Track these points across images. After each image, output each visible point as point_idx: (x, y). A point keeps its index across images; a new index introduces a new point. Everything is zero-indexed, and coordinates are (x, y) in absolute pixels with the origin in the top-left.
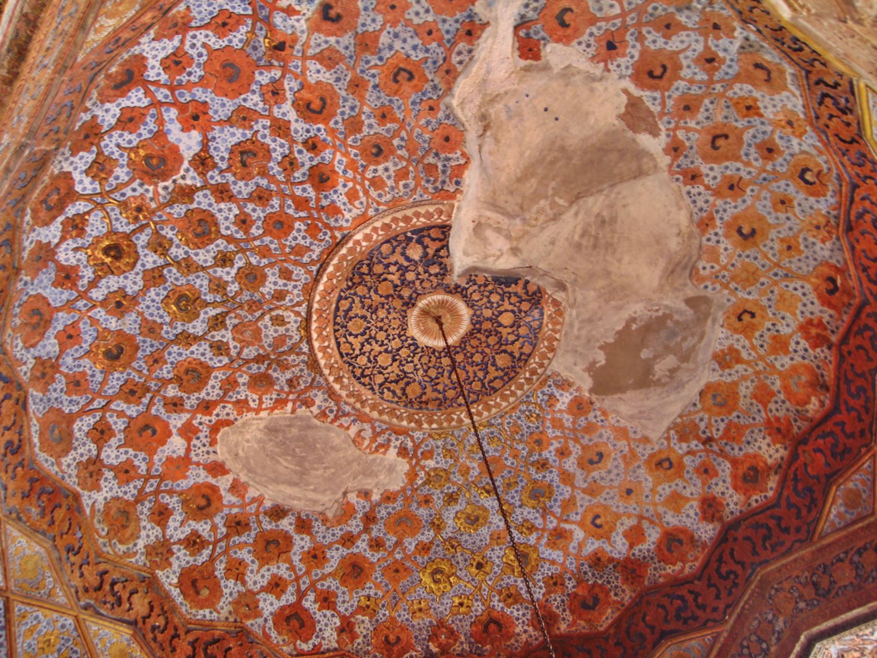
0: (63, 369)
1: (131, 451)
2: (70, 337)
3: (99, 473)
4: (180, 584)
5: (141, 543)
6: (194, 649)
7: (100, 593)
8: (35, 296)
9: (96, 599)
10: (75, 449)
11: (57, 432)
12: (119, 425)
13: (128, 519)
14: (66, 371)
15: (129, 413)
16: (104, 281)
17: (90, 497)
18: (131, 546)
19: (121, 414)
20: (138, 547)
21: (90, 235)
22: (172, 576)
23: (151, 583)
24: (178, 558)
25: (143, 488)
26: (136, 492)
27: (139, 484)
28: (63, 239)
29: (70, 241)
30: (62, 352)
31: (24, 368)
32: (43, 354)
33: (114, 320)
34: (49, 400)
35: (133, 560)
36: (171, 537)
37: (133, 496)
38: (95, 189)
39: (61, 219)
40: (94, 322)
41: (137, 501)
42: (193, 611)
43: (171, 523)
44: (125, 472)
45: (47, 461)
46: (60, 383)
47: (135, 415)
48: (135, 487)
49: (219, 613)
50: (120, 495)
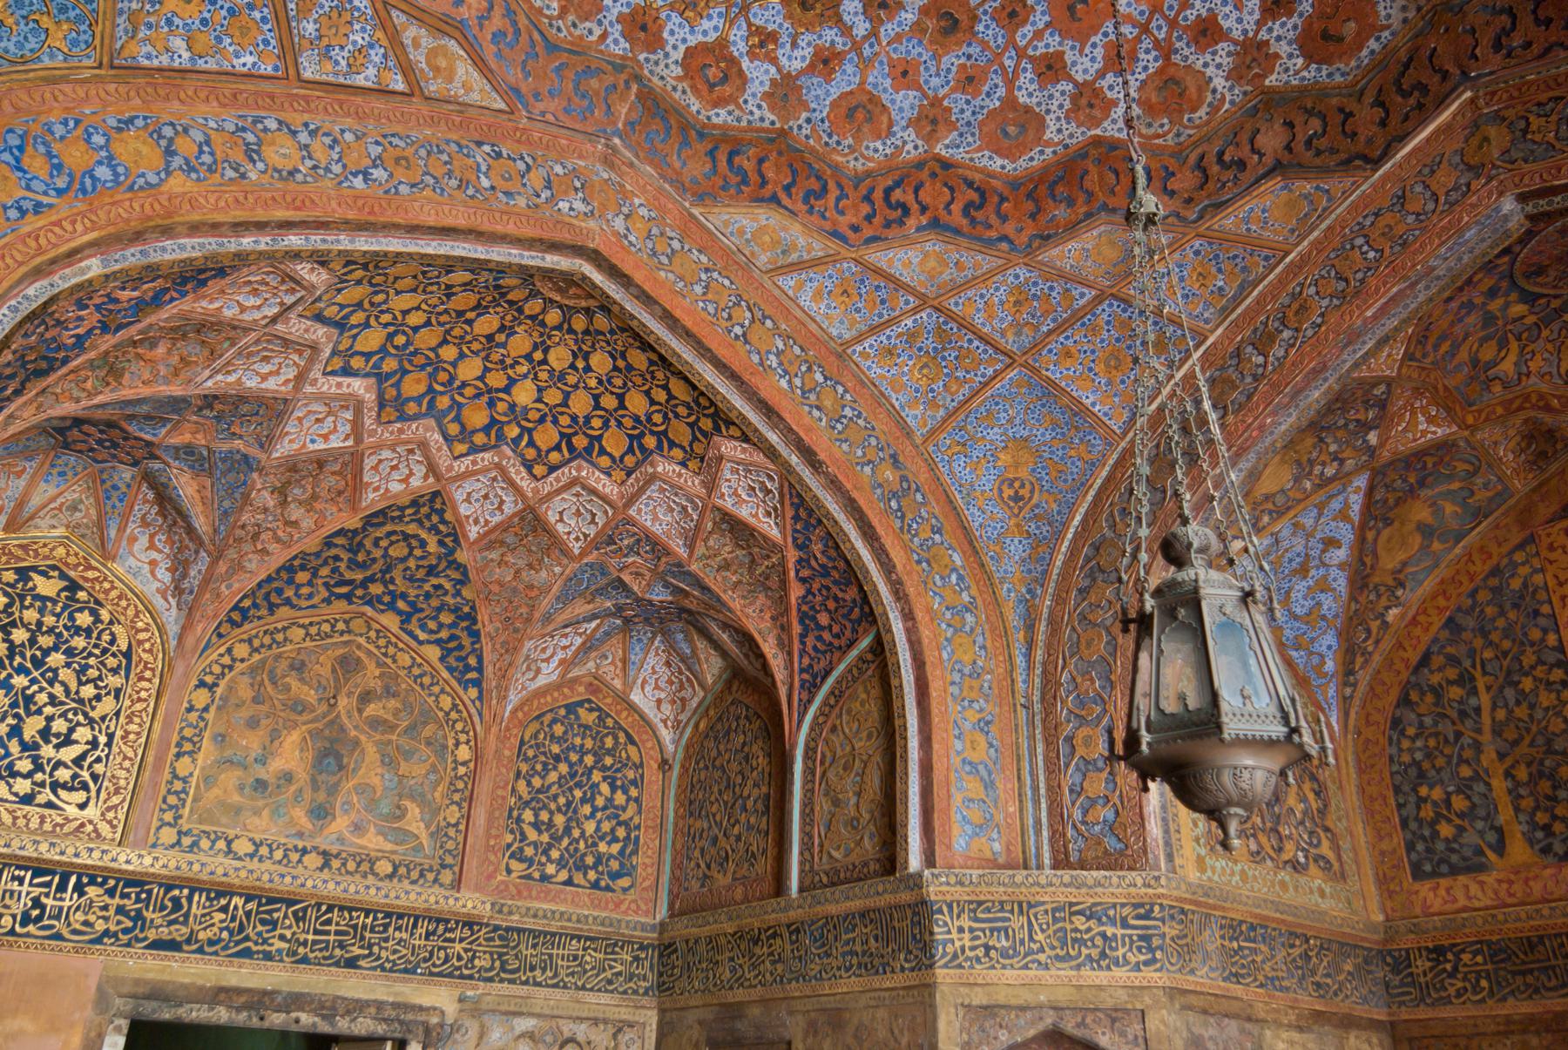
0: (941, 93)
1: (1096, 39)
2: (905, 73)
3: (1098, 93)
4: (1309, 58)
5: (1219, 82)
6: (1382, 104)
7: (1210, 185)
8: (831, 110)
9: (1209, 196)
10: (1048, 112)
11: (1011, 130)
12: (1052, 42)
13: (1177, 83)
14: (947, 88)
15: (1041, 25)
16: (846, 18)
17: (1114, 121)
18: (1209, 98)
19: (1038, 35)
20: (1220, 89)
21: (781, 25)
22: (1290, 64)
23: (1269, 103)
24: (1279, 38)
25: (1157, 42)
26: (1154, 53)
27: (1146, 43)
28: (774, 61)
29: (780, 52)
30: (919, 88)
31: (909, 147)
32: (907, 114)
33: (903, 14)
34: (969, 124)
35: (1227, 106)
36: (1245, 32)
37: (1156, 60)
38: (720, 14)
39: (745, 63)
40: (898, 38)
41: (1167, 58)
42: (1353, 63)
43: (1225, 24)
44: (1118, 59)
45: (1032, 159)
46: (957, 103)
47: (1047, 18)
48: (1147, 52)
49: (1388, 27)
50: (1143, 76)
